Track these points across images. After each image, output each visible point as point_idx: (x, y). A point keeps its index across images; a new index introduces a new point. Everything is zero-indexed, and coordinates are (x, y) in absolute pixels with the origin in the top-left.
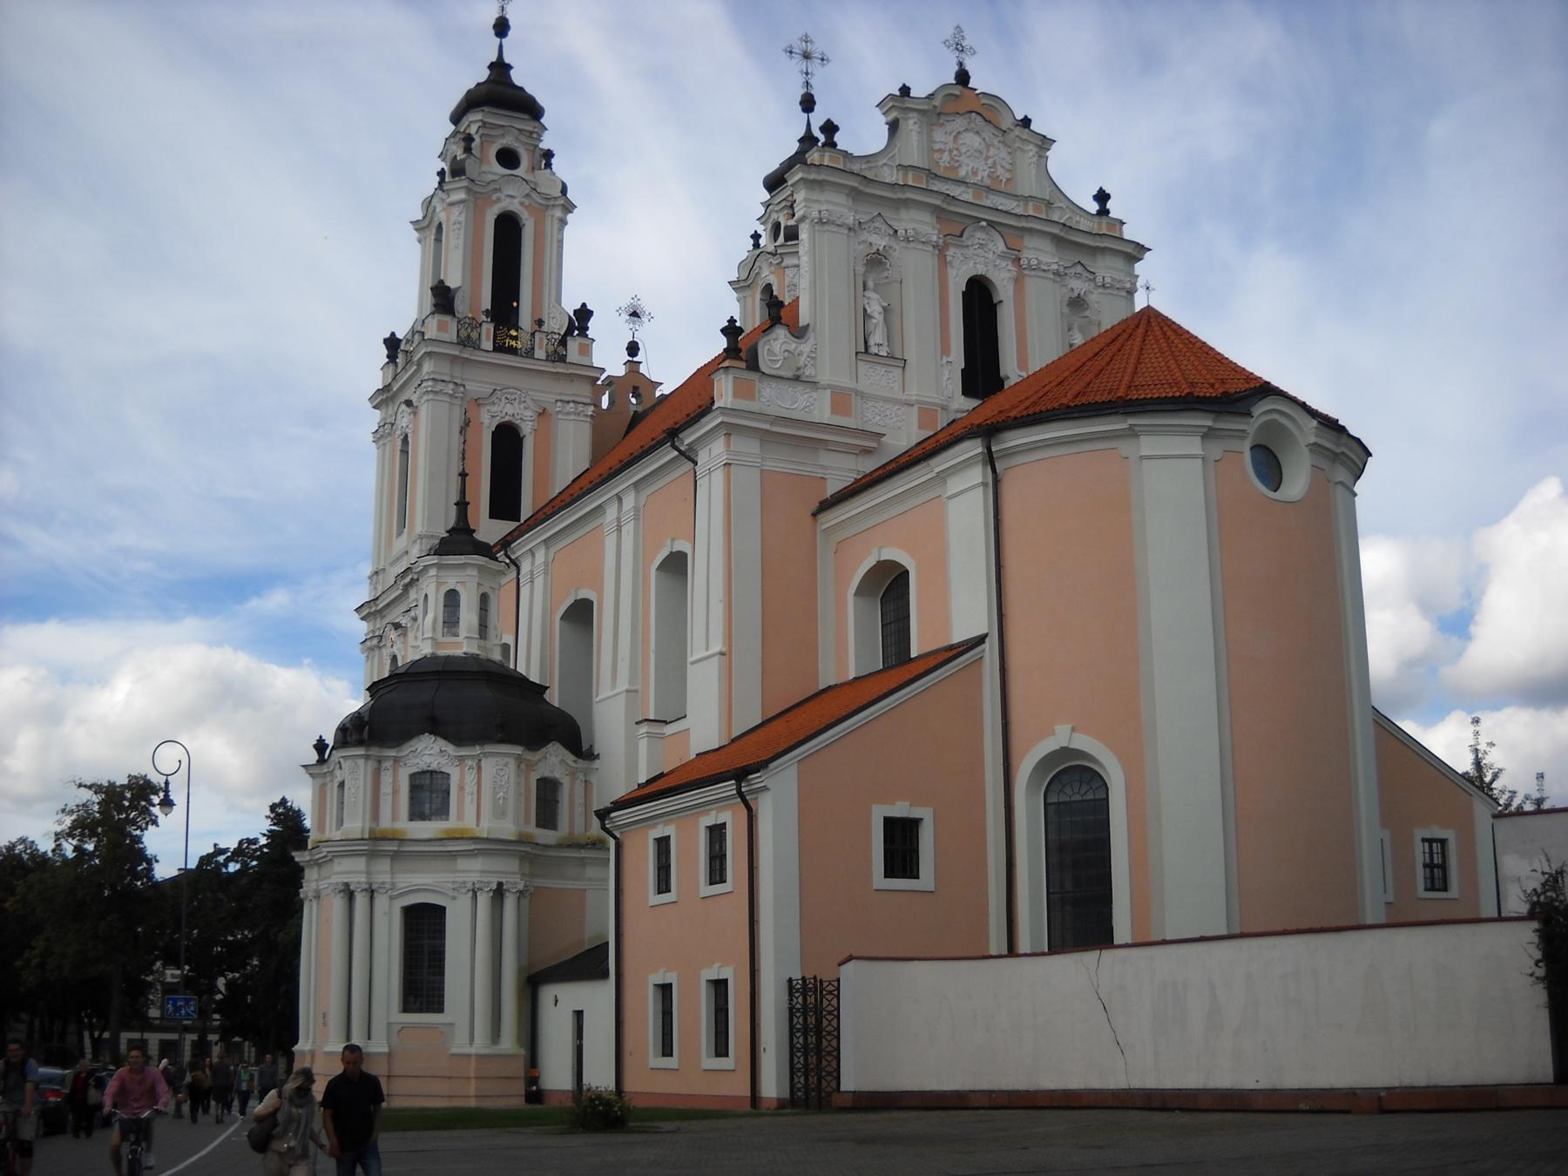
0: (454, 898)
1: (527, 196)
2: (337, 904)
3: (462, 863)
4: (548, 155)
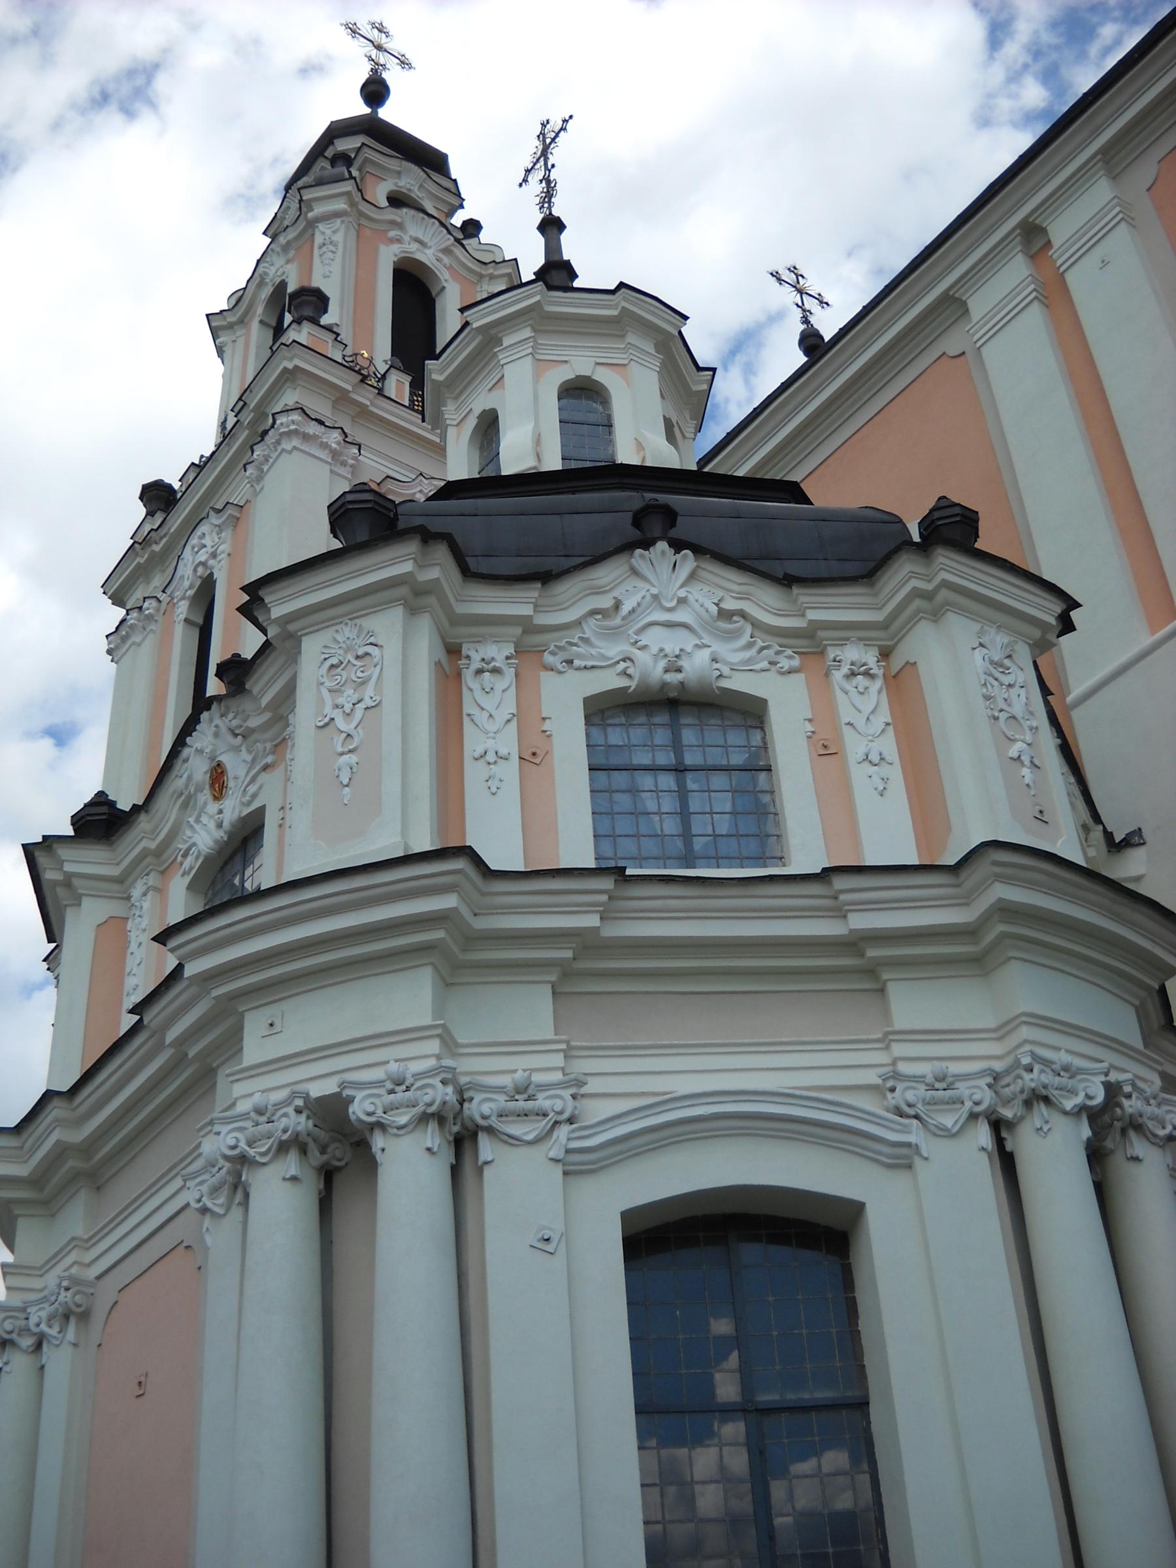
0: (903, 1159)
1: (447, 251)
2: (281, 1200)
3: (913, 1004)
4: (472, 227)
